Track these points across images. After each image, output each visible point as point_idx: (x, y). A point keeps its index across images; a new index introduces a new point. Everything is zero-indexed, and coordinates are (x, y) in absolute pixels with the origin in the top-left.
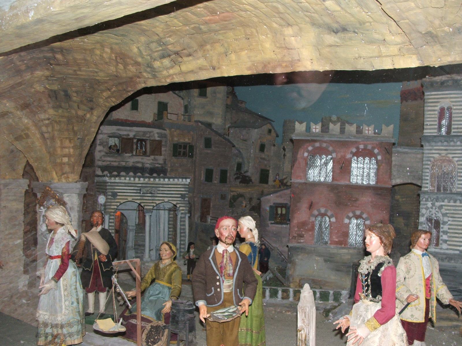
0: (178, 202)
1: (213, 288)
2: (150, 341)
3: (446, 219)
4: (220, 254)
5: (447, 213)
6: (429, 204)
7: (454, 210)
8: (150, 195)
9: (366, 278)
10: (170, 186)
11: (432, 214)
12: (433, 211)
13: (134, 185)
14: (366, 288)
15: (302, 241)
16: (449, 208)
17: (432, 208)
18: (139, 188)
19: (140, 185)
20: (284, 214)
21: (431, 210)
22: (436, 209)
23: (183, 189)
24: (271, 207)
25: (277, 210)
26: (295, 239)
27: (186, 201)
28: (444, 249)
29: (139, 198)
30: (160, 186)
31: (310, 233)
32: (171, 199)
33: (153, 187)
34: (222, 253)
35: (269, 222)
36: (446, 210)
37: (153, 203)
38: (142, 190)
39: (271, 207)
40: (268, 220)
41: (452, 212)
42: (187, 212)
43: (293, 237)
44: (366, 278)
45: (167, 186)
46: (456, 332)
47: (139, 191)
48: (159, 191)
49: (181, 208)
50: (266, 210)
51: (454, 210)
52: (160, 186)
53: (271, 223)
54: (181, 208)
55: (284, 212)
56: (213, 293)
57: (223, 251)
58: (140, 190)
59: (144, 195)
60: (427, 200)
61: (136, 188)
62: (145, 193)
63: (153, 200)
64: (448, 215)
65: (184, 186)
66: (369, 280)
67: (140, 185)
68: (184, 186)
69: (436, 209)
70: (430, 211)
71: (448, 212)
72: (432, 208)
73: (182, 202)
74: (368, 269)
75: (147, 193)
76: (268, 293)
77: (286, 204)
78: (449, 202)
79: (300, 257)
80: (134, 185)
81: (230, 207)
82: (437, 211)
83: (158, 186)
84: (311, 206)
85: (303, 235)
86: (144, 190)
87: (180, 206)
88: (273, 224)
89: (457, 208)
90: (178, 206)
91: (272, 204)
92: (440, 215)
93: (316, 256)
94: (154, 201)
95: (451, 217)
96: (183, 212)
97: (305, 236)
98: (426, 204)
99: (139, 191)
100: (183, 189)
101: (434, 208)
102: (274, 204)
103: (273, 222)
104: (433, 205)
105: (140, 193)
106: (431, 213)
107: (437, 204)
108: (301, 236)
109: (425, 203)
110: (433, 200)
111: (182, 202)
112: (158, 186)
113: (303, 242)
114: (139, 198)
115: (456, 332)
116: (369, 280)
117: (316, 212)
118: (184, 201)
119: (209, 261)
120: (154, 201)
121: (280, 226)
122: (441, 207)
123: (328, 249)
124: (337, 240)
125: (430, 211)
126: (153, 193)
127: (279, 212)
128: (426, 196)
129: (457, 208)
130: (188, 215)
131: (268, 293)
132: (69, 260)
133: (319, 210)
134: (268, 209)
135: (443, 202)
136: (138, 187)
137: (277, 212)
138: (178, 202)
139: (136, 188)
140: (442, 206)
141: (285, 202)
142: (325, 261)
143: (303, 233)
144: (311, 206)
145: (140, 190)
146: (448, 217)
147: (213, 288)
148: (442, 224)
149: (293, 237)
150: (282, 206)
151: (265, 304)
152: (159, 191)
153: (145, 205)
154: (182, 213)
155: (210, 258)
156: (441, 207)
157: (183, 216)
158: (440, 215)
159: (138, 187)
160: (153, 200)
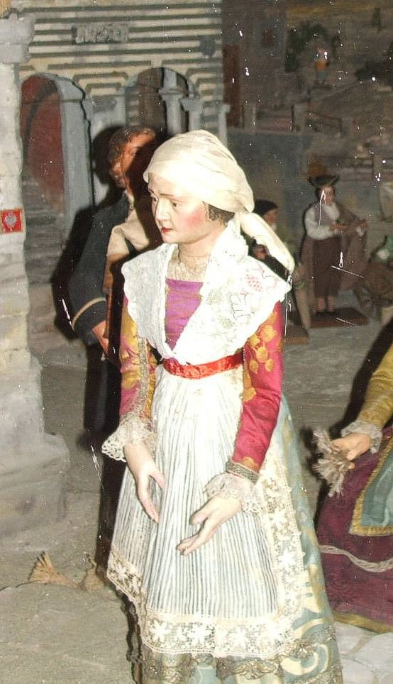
0: (194, 66)
8: (105, 47)
10: (164, 12)
13: (52, 15)
18: (69, 26)
19: (71, 15)
23: (205, 21)
27: (217, 60)
29: (70, 60)
30: (137, 13)
32: (170, 56)
33: (114, 19)
37: (115, 74)
38: (79, 32)
42: (221, 98)
45: (157, 13)
47: (69, 37)
48: (133, 30)
49: (203, 87)
52: (137, 13)
54: (203, 87)
58: (74, 31)
59: (85, 48)
61: (60, 26)
62: (90, 43)
63: (116, 64)
65: (207, 10)
67: (71, 15)
68: (207, 10)
73: (206, 65)
75: (97, 43)
80: (52, 15)
81: (288, 70)
83: (129, 13)
86: (85, 32)
87: (200, 81)
90: (193, 79)
94: (118, 70)
96: (209, 98)
99: (69, 37)
100: (205, 21)
105: (74, 43)
111: (206, 65)
112: (129, 13)
114: (70, 60)
118: (211, 60)
120: (118, 70)
126: (116, 39)
130: (225, 108)
132: (272, 372)
136: (65, 21)
138: (194, 66)
139: (60, 26)
145: (74, 31)
152: (133, 30)
153: (90, 87)
154: (207, 104)
157: (208, 112)
159: (65, 21)
160: (116, 64)
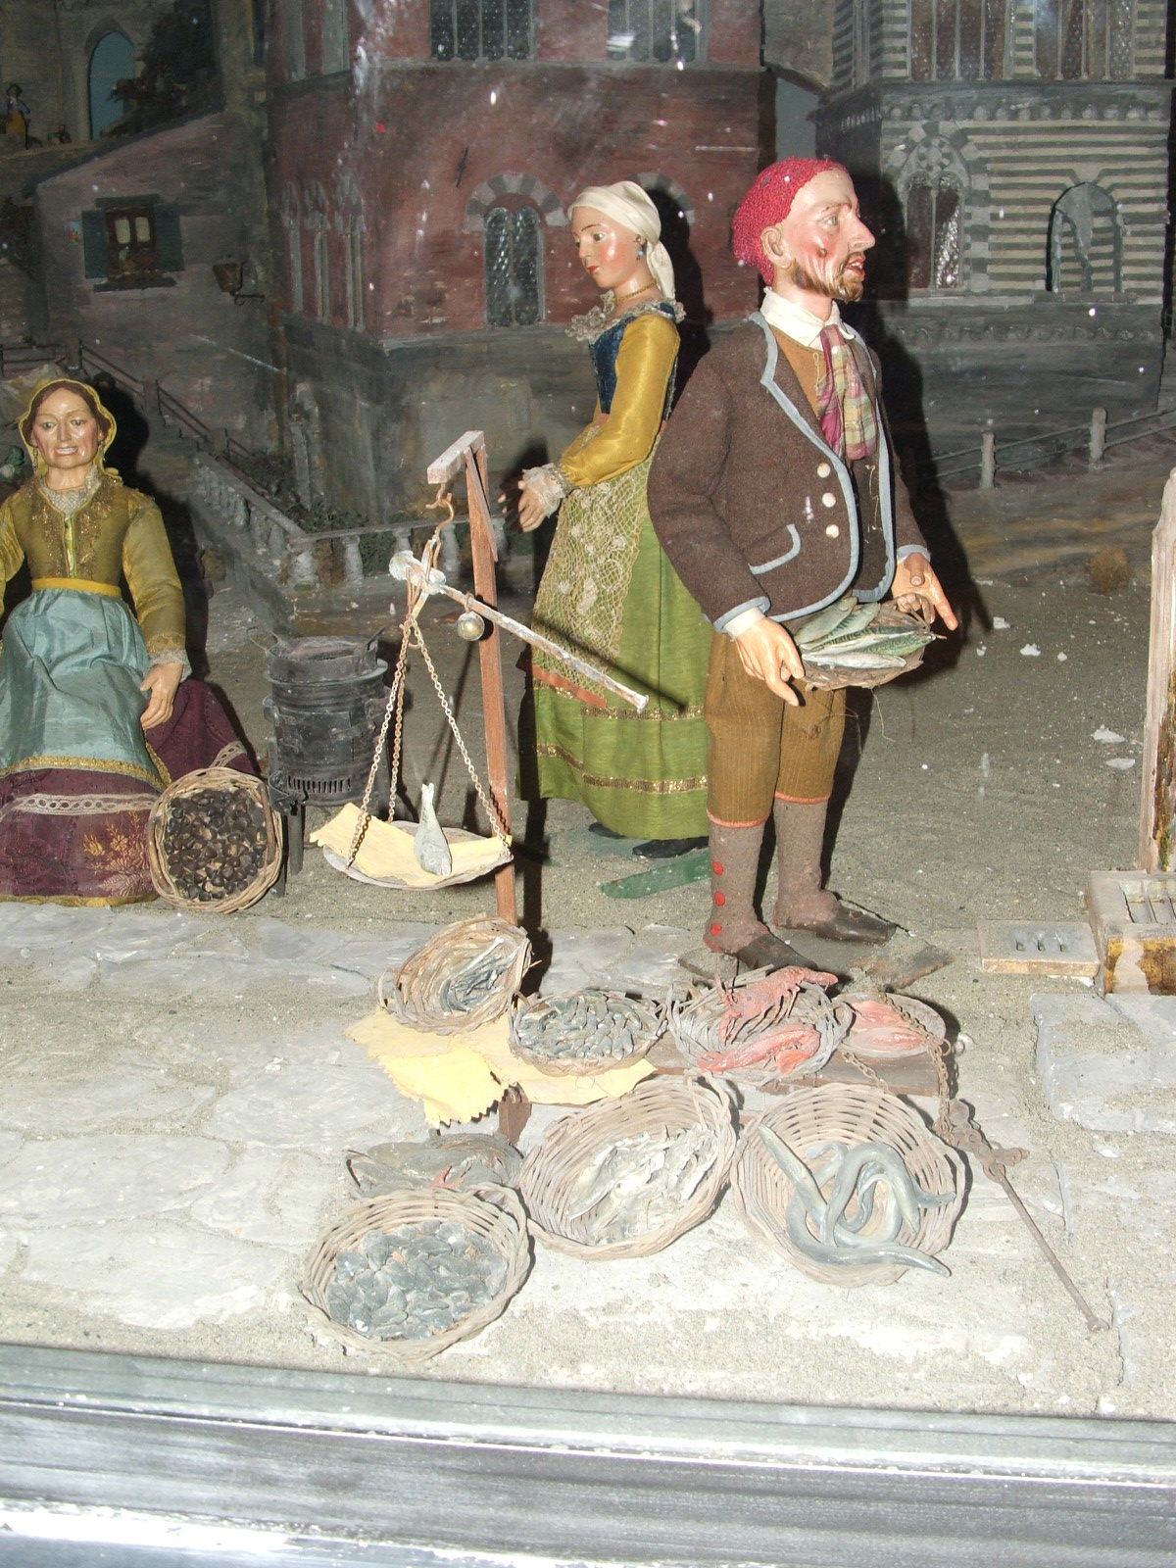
1: (791, 529)
2: (202, 873)
3: (981, 183)
4: (810, 351)
5: (987, 160)
6: (917, 131)
7: (1011, 146)
11: (930, 168)
12: (935, 155)
15: (437, 320)
16: (992, 139)
17: (927, 145)
20: (144, 244)
21: (923, 150)
22: (941, 145)
24: (87, 217)
25: (112, 229)
26: (408, 314)
28: (977, 295)
31: (468, 283)
34: (818, 345)
35: (88, 284)
36: (981, 146)
39: (87, 217)
40: (82, 272)
41: (1003, 153)
43: (400, 306)
46: (1072, 580)
50: (69, 234)
51: (1011, 146)
53: (98, 288)
55: (144, 235)
56: (795, 551)
57: (823, 334)
60: (908, 115)
64: (989, 166)
69: (941, 145)
70: (922, 158)
71: (986, 154)
72: (927, 145)
76: (353, 557)
77: (154, 198)
78: (992, 117)
79: (435, 388)
82: (947, 156)
84: (462, 169)
85: (441, 293)
88: (106, 288)
89: (1021, 138)
91: (91, 206)
92: (957, 168)
93: (499, 375)
95: (1001, 174)
97: (447, 296)
98: (906, 131)
101: (936, 142)
102: (99, 202)
103: (104, 281)
104: (931, 130)
106: (924, 164)
107: (947, 127)
108: (435, 300)
109: (898, 125)
110: (931, 111)
113: (443, 324)
115: (1072, 580)
117: (485, 194)
119: (763, 389)
121: (136, 293)
122: (961, 138)
123: (545, 342)
124: (575, 300)
125: (922, 158)
127: (124, 237)
128: (906, 100)
129: (1021, 138)
131: (353, 557)
133: (496, 184)
134: (76, 227)
135: (970, 117)
137: (114, 238)
140: (965, 132)
141: (146, 191)
142: (539, 390)
143: (440, 285)
144: (462, 169)
146: (991, 174)
147: (791, 529)
148: (968, 202)
149: (400, 306)
150: (133, 208)
151: (355, 605)
155: (768, 379)
156: (961, 138)
158: (957, 168)
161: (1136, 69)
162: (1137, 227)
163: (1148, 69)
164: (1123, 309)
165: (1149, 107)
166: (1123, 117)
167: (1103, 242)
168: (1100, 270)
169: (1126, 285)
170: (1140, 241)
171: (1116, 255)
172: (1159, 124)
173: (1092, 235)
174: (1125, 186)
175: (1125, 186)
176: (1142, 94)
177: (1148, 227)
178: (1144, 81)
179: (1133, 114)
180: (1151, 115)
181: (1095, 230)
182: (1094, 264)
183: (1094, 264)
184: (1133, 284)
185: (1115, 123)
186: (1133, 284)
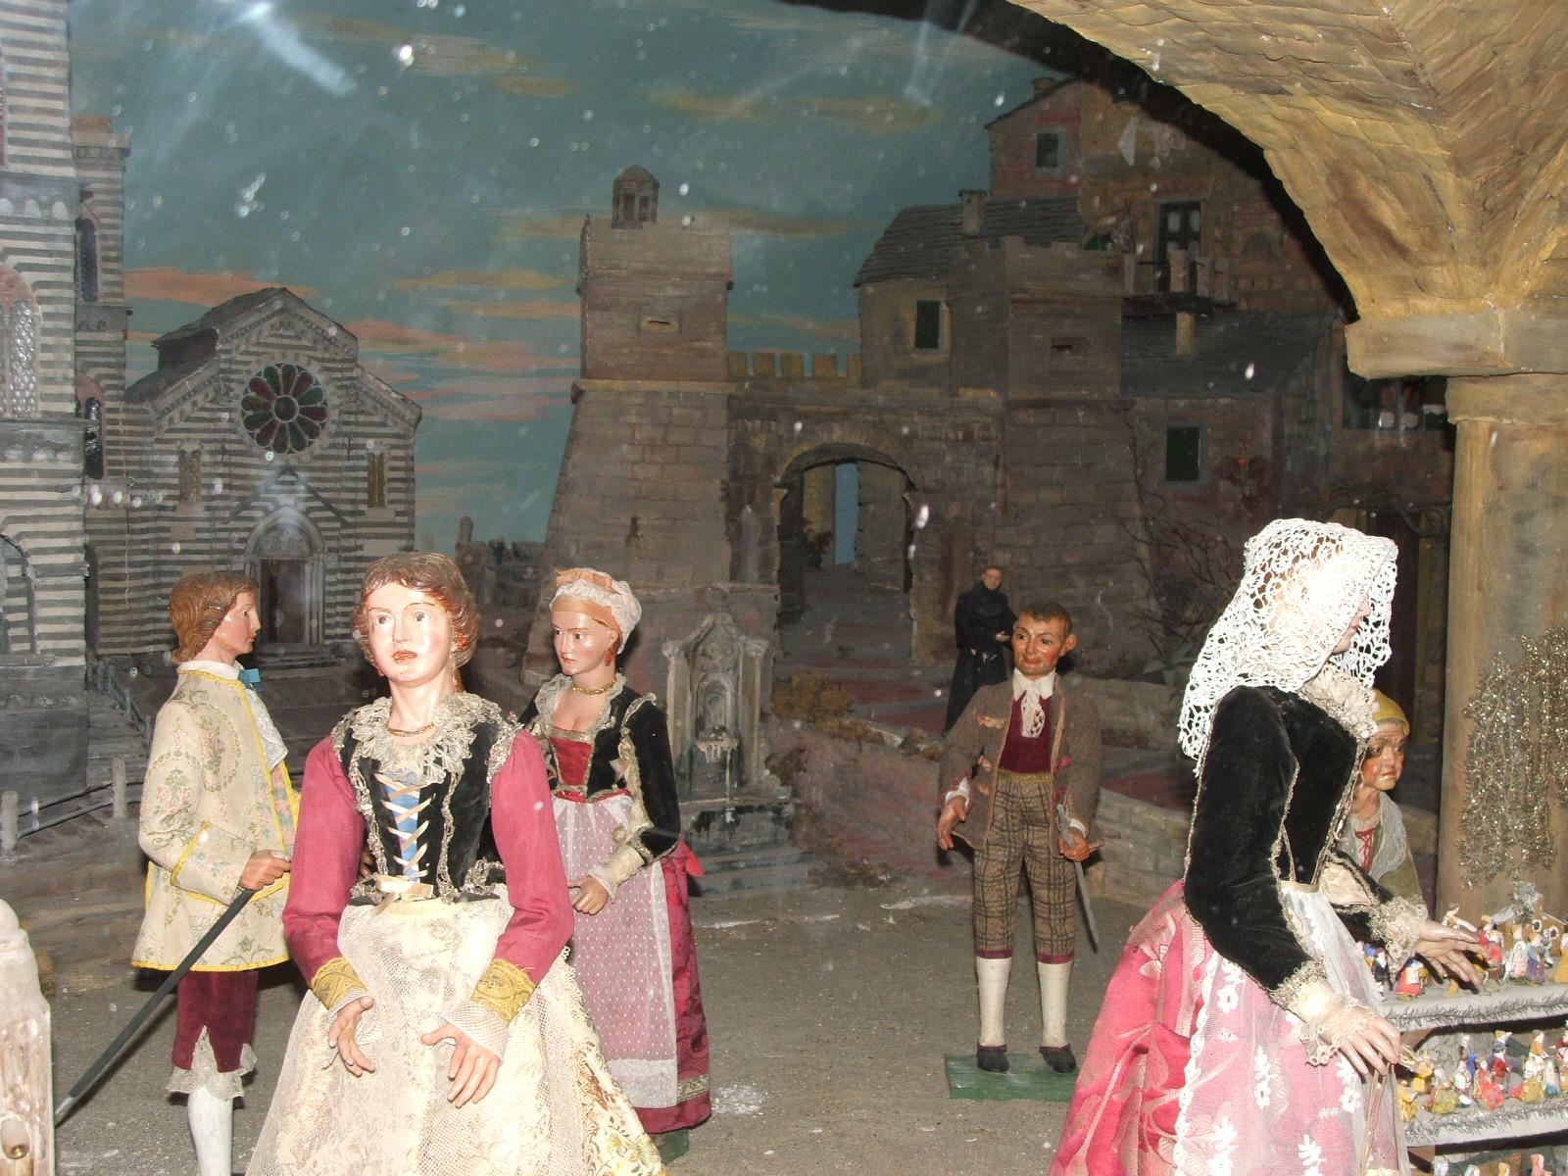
9: (427, 802)
14: (424, 848)
44: (427, 802)
66: (446, 810)
74: (438, 761)
116: (446, 810)
161: (42, 406)
162: (51, 581)
163: (56, 407)
164: (37, 673)
165: (58, 448)
166: (28, 459)
167: (18, 594)
168: (16, 624)
169: (42, 645)
170: (54, 595)
171: (29, 608)
172: (73, 467)
173: (6, 586)
174: (36, 534)
175: (36, 534)
176: (50, 434)
177: (65, 580)
178: (50, 420)
179: (40, 456)
180: (61, 456)
181: (10, 580)
182: (11, 617)
183: (11, 617)
184: (49, 644)
185: (19, 465)
186: (49, 644)
